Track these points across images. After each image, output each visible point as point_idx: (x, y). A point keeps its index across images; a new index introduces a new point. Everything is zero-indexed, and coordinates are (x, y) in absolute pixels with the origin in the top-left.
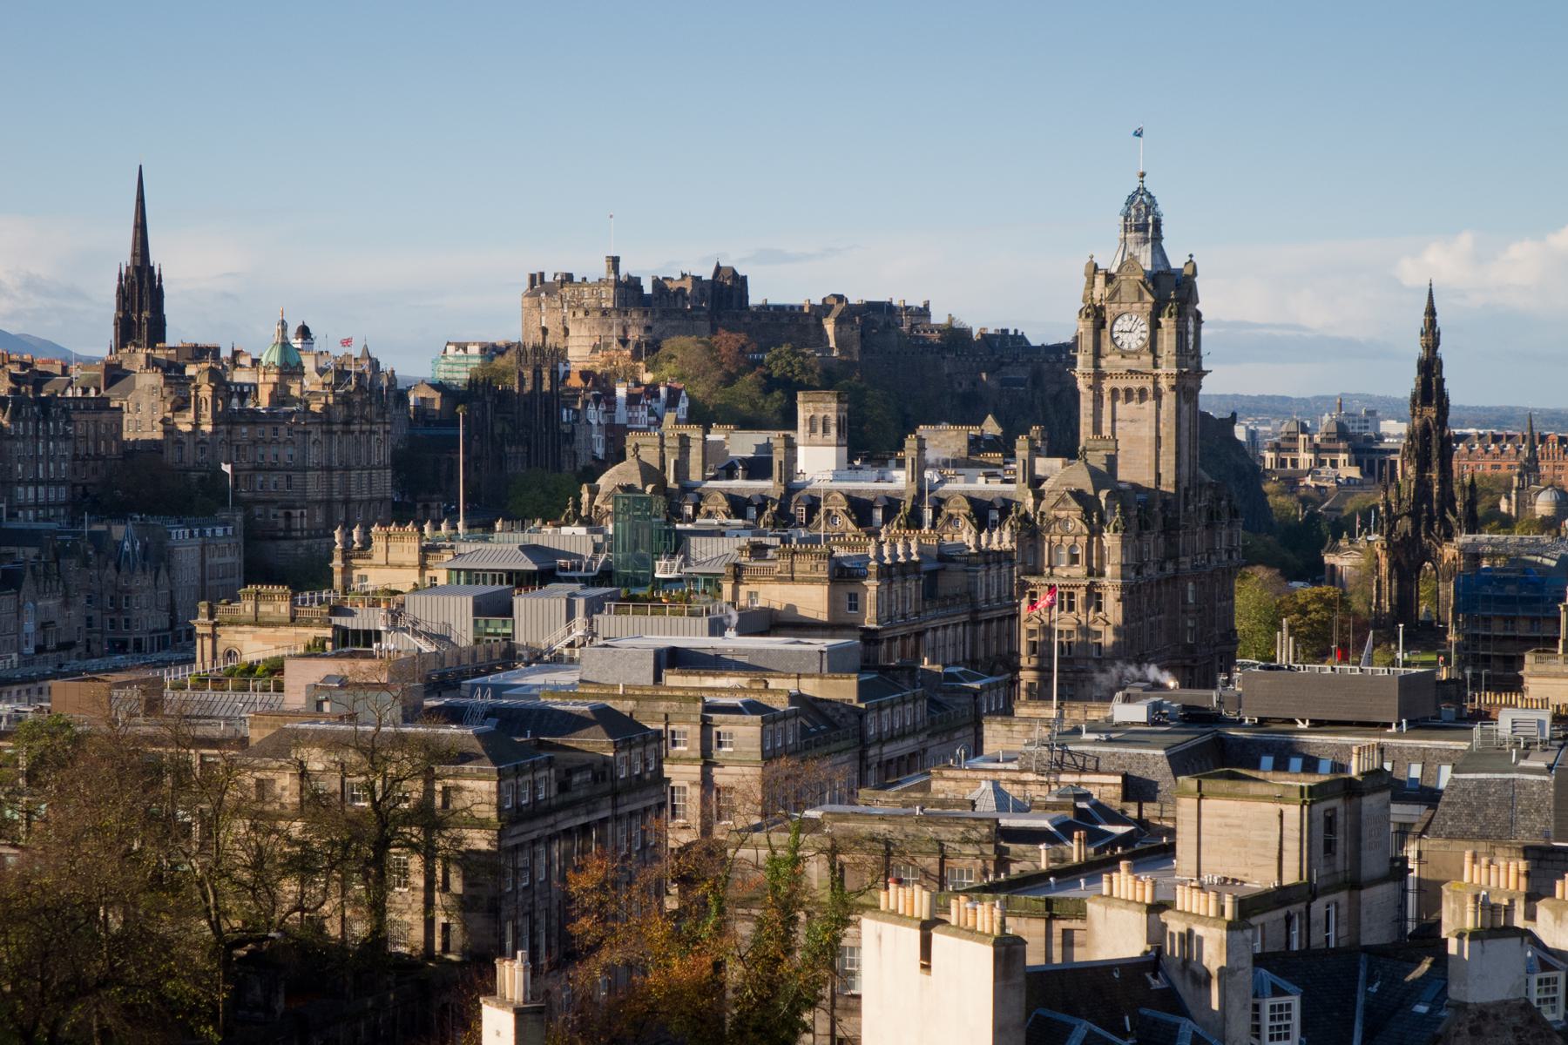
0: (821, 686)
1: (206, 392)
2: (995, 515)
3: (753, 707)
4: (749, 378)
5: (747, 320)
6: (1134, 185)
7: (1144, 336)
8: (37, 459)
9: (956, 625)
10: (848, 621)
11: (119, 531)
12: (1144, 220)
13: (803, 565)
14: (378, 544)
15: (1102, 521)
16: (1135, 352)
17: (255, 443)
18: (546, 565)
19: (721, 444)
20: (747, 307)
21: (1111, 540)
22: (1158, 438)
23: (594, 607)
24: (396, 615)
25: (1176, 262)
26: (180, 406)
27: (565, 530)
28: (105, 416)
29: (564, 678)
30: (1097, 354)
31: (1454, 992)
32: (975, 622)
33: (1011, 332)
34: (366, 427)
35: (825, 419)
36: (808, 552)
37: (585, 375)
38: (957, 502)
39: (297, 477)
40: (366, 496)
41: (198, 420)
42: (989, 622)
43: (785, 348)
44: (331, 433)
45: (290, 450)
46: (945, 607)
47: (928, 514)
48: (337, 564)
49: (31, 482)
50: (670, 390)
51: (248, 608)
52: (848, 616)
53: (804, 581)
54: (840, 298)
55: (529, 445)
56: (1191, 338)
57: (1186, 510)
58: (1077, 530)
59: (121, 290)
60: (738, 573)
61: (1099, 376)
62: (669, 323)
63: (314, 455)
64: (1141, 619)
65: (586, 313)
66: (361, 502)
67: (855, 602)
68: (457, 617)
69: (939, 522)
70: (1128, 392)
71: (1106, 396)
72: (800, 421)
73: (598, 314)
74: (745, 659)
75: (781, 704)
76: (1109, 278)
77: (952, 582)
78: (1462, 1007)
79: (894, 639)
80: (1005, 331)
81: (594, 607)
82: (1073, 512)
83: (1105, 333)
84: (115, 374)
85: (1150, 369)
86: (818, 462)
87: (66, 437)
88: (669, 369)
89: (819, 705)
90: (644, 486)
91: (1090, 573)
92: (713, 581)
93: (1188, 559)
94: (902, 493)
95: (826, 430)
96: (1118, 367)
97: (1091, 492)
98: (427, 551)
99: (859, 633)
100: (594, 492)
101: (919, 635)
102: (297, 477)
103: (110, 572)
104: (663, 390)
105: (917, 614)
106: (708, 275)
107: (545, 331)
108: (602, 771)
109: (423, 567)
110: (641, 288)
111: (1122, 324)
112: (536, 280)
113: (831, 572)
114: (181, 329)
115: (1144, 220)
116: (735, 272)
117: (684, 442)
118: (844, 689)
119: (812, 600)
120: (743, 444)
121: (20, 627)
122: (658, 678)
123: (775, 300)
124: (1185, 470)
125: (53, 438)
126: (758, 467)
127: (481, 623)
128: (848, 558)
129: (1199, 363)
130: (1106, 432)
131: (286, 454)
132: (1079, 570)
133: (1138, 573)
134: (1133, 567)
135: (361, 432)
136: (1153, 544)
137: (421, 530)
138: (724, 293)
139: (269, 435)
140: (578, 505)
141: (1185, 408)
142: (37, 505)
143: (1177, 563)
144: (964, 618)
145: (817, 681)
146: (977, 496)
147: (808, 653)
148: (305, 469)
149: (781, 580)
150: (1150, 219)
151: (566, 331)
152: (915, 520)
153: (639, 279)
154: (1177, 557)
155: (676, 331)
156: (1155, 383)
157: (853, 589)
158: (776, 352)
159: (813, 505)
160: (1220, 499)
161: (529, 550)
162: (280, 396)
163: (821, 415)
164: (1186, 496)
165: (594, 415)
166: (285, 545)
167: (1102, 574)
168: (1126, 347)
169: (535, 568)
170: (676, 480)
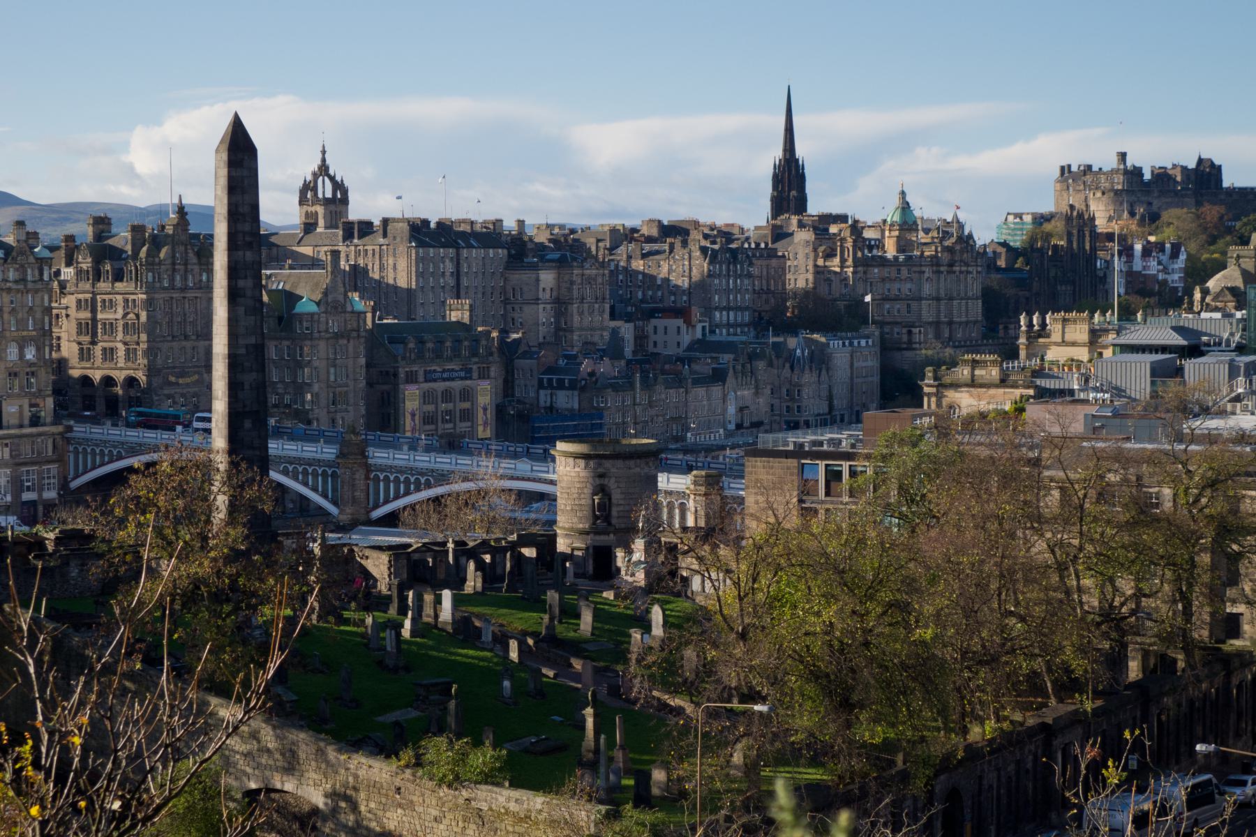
5: (1223, 197)
8: (728, 291)
11: (792, 342)
17: (883, 280)
18: (1193, 342)
26: (829, 255)
28: (774, 262)
34: (964, 269)
39: (914, 305)
40: (964, 319)
44: (939, 272)
45: (909, 285)
49: (724, 308)
51: (965, 372)
59: (775, 176)
62: (1164, 200)
63: (927, 289)
65: (1103, 193)
66: (960, 323)
68: (1136, 376)
87: (749, 276)
98: (1095, 334)
102: (914, 305)
103: (786, 372)
104: (1168, 246)
106: (1192, 165)
112: (1065, 170)
121: (725, 410)
125: (740, 276)
131: (906, 288)
135: (961, 272)
137: (1092, 317)
138: (1205, 176)
139: (894, 275)
140: (1191, 303)
142: (729, 325)
148: (921, 299)
155: (1169, 206)
158: (1245, 220)
161: (1179, 330)
166: (908, 354)
169: (1185, 343)
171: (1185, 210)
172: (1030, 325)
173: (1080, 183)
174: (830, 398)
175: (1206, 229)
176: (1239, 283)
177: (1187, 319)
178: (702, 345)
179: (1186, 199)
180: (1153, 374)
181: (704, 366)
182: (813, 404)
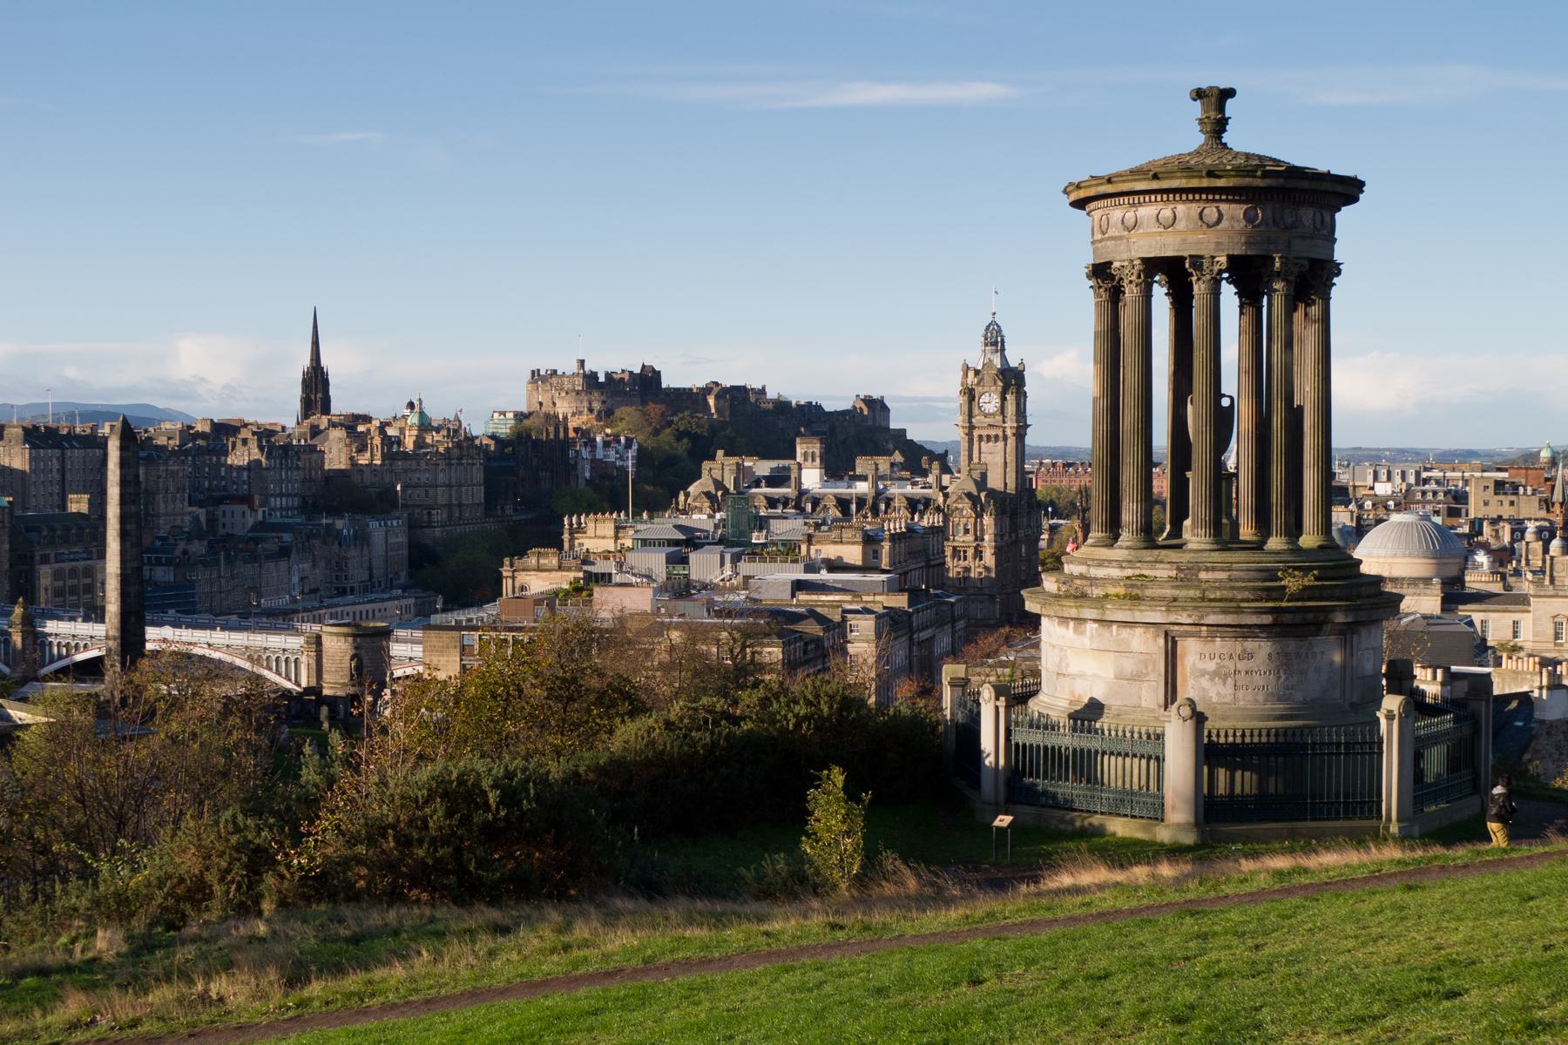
1: (377, 441)
3: (869, 611)
4: (668, 431)
8: (281, 481)
11: (339, 524)
12: (995, 339)
13: (847, 534)
14: (591, 525)
17: (406, 471)
21: (988, 520)
23: (736, 559)
24: (620, 565)
25: (1013, 363)
26: (361, 450)
28: (315, 456)
31: (1537, 715)
32: (928, 566)
37: (576, 430)
39: (431, 491)
41: (372, 457)
47: (883, 507)
48: (566, 536)
50: (627, 439)
54: (717, 384)
59: (304, 380)
60: (810, 539)
63: (441, 478)
67: (876, 555)
70: (989, 437)
78: (1542, 722)
81: (736, 559)
82: (966, 506)
83: (975, 404)
84: (315, 431)
86: (812, 478)
87: (298, 468)
88: (621, 426)
98: (618, 529)
100: (687, 495)
102: (431, 491)
103: (335, 547)
104: (623, 439)
106: (637, 370)
108: (818, 641)
109: (617, 538)
111: (985, 398)
114: (342, 402)
115: (995, 339)
118: (901, 601)
120: (763, 468)
121: (290, 580)
122: (793, 596)
126: (777, 479)
131: (425, 477)
132: (970, 537)
134: (999, 536)
138: (648, 381)
139: (414, 466)
142: (281, 509)
149: (835, 543)
152: (875, 511)
155: (621, 404)
159: (816, 501)
161: (679, 527)
162: (420, 442)
165: (585, 453)
166: (428, 531)
172: (571, 524)
174: (370, 568)
176: (712, 489)
177: (683, 520)
178: (261, 526)
180: (668, 562)
181: (272, 546)
182: (358, 574)
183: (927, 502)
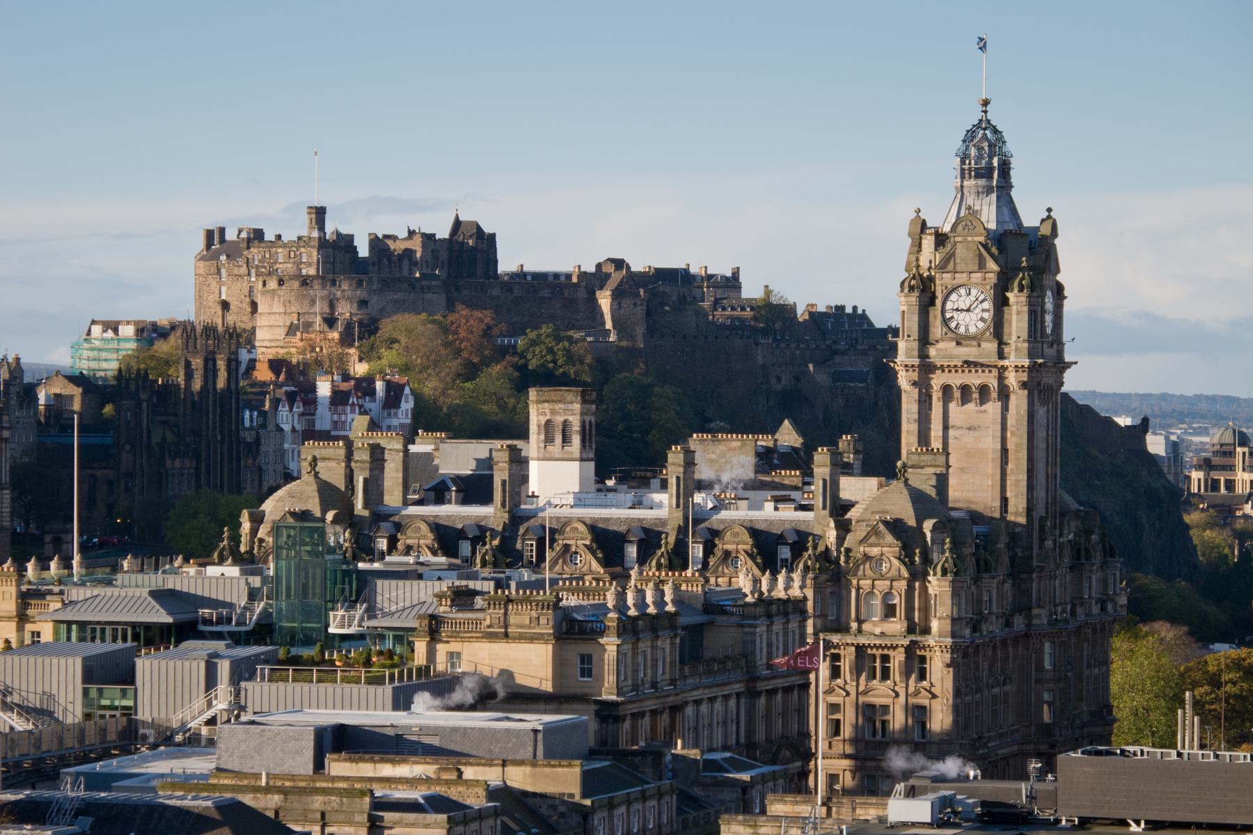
0: (533, 776)
2: (785, 552)
3: (437, 804)
4: (496, 369)
6: (975, 116)
7: (986, 315)
9: (726, 698)
10: (579, 691)
13: (520, 618)
15: (927, 561)
16: (974, 338)
19: (428, 457)
20: (495, 275)
21: (938, 585)
22: (1004, 451)
25: (1030, 217)
27: (212, 571)
29: (198, 765)
30: (924, 340)
33: (849, 310)
35: (566, 424)
36: (526, 600)
37: (276, 365)
38: (736, 535)
42: (772, 692)
43: (545, 329)
46: (710, 672)
47: (696, 550)
50: (389, 386)
52: (578, 684)
53: (522, 638)
54: (619, 264)
55: (198, 458)
56: (1049, 318)
57: (1041, 546)
58: (893, 573)
60: (434, 627)
61: (926, 368)
64: (979, 690)
67: (588, 666)
68: (62, 685)
69: (712, 561)
70: (965, 389)
71: (936, 395)
72: (533, 428)
73: (296, 284)
74: (435, 741)
75: (476, 800)
76: (941, 239)
77: (721, 640)
79: (642, 714)
80: (840, 308)
82: (888, 548)
83: (935, 313)
85: (994, 359)
86: (556, 481)
88: (389, 356)
89: (530, 801)
90: (324, 512)
91: (911, 630)
92: (403, 636)
93: (1043, 612)
94: (663, 522)
95: (566, 440)
96: (951, 357)
97: (912, 522)
98: (27, 598)
99: (594, 707)
100: (257, 520)
101: (676, 709)
104: (379, 386)
105: (673, 682)
106: (443, 232)
107: (225, 305)
109: (22, 618)
110: (354, 250)
111: (955, 301)
112: (214, 237)
113: (557, 627)
115: (988, 163)
116: (479, 228)
117: (377, 453)
118: (563, 781)
119: (533, 663)
120: (458, 457)
122: (319, 765)
123: (534, 265)
124: (1040, 494)
126: (475, 488)
127: (93, 693)
128: (579, 608)
129: (1060, 352)
130: (936, 444)
132: (896, 626)
133: (975, 629)
134: (968, 621)
136: (997, 590)
137: (21, 571)
138: (465, 256)
140: (236, 539)
141: (1041, 411)
143: (1029, 617)
144: (738, 687)
145: (528, 769)
146: (762, 527)
147: (518, 733)
149: (491, 637)
150: (995, 162)
151: (254, 306)
152: (678, 559)
153: (351, 237)
154: (1030, 609)
155: (400, 307)
156: (1001, 378)
157: (585, 648)
158: (532, 335)
160: (1089, 533)
161: (163, 596)
163: (559, 419)
164: (1042, 528)
167: (926, 631)
168: (962, 330)
169: (170, 620)
170: (366, 505)
171: (423, 316)
173: (241, 261)
175: (458, 352)
176: (315, 508)
179: (430, 296)
183: (801, 540)
